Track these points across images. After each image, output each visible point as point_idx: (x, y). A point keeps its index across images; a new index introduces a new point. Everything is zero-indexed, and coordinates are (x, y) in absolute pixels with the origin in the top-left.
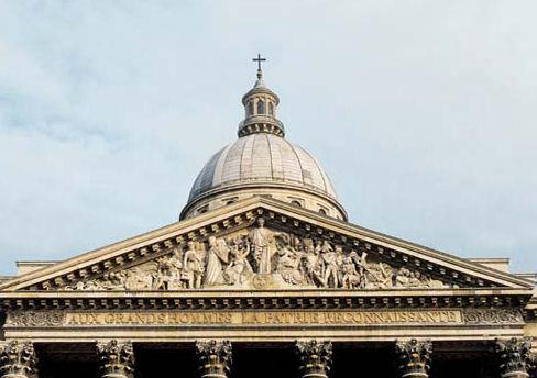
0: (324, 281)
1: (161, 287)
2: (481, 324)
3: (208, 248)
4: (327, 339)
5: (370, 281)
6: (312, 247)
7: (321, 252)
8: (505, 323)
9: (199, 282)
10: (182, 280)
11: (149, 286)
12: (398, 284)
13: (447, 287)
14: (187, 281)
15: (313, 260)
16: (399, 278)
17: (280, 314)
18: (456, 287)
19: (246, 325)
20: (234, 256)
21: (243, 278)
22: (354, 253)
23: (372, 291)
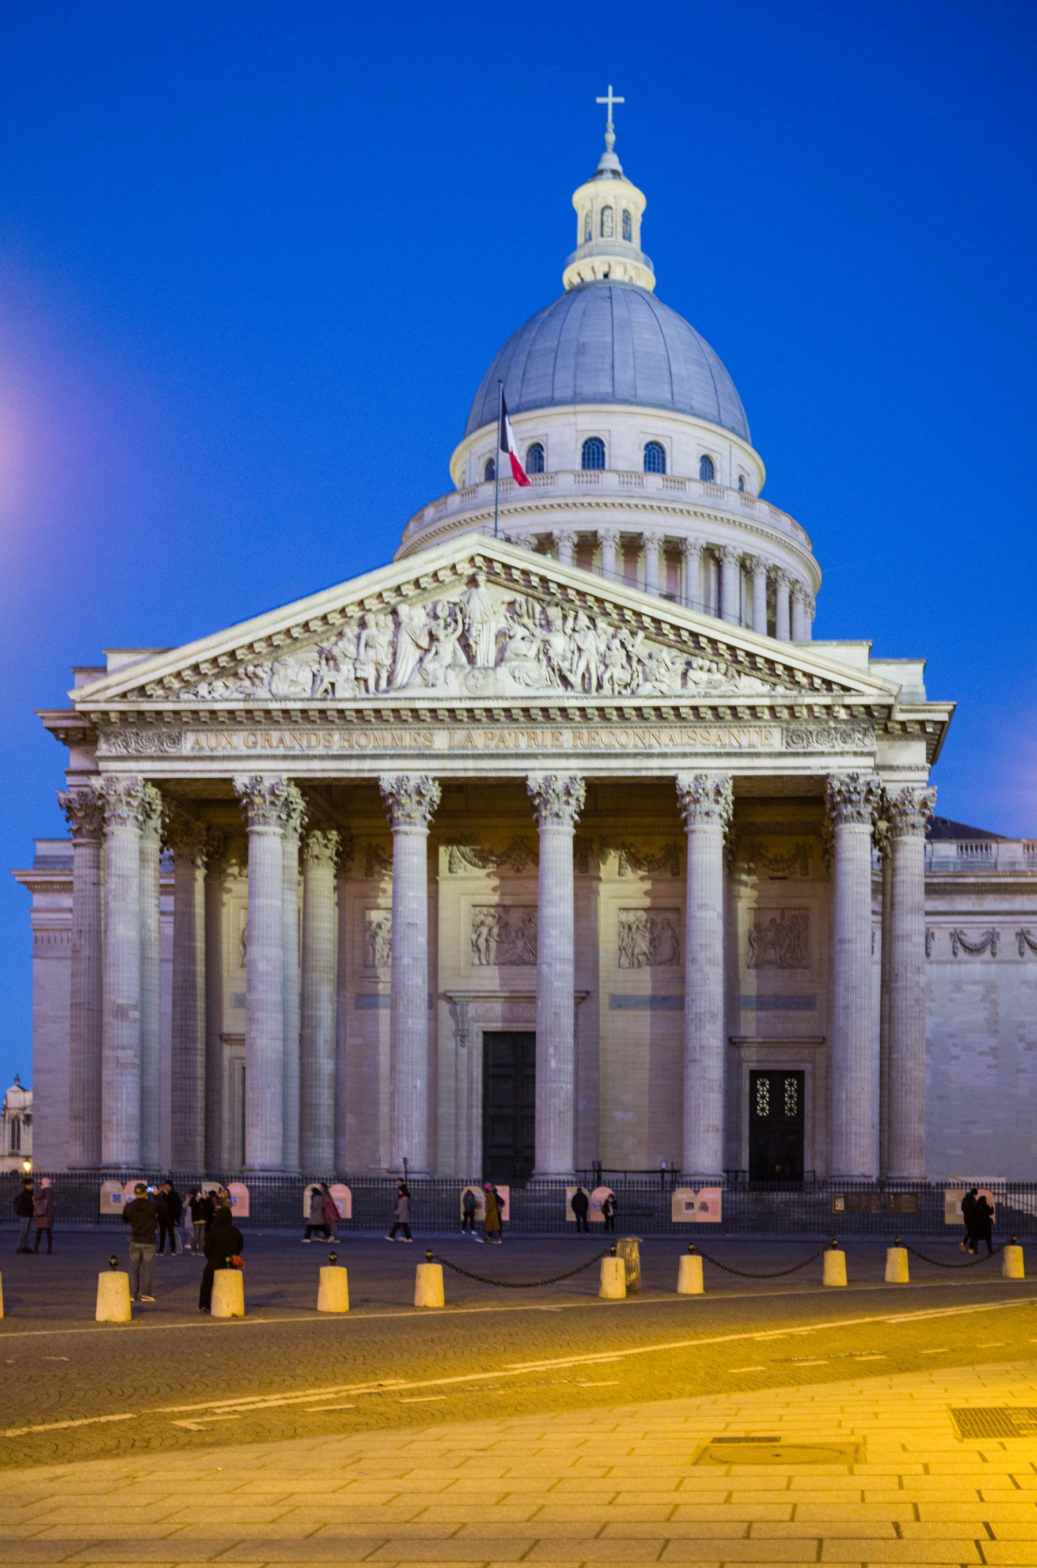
0: (575, 679)
1: (326, 691)
2: (809, 750)
3: (398, 624)
4: (571, 773)
5: (646, 680)
6: (559, 623)
7: (574, 630)
8: (847, 748)
9: (383, 684)
10: (357, 679)
11: (309, 690)
12: (690, 684)
13: (766, 688)
14: (366, 681)
15: (559, 644)
16: (691, 674)
17: (506, 732)
18: (780, 689)
19: (456, 752)
20: (437, 640)
21: (451, 673)
22: (624, 633)
23: (646, 697)
